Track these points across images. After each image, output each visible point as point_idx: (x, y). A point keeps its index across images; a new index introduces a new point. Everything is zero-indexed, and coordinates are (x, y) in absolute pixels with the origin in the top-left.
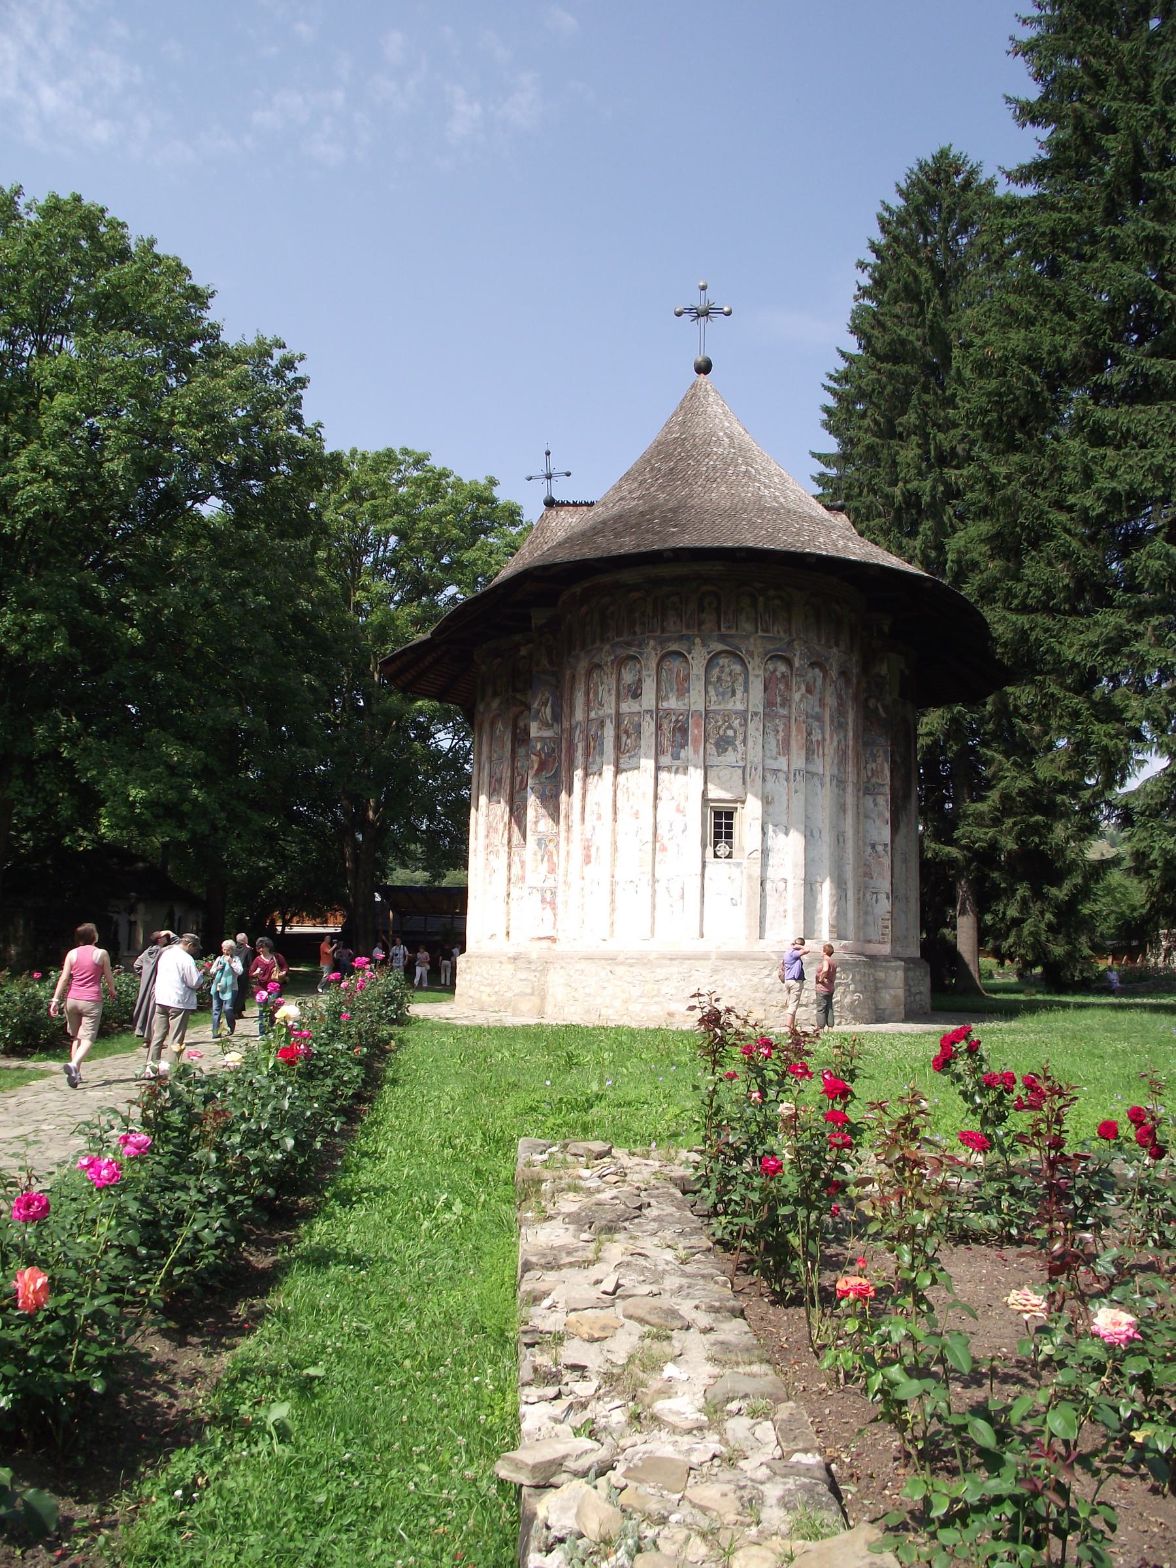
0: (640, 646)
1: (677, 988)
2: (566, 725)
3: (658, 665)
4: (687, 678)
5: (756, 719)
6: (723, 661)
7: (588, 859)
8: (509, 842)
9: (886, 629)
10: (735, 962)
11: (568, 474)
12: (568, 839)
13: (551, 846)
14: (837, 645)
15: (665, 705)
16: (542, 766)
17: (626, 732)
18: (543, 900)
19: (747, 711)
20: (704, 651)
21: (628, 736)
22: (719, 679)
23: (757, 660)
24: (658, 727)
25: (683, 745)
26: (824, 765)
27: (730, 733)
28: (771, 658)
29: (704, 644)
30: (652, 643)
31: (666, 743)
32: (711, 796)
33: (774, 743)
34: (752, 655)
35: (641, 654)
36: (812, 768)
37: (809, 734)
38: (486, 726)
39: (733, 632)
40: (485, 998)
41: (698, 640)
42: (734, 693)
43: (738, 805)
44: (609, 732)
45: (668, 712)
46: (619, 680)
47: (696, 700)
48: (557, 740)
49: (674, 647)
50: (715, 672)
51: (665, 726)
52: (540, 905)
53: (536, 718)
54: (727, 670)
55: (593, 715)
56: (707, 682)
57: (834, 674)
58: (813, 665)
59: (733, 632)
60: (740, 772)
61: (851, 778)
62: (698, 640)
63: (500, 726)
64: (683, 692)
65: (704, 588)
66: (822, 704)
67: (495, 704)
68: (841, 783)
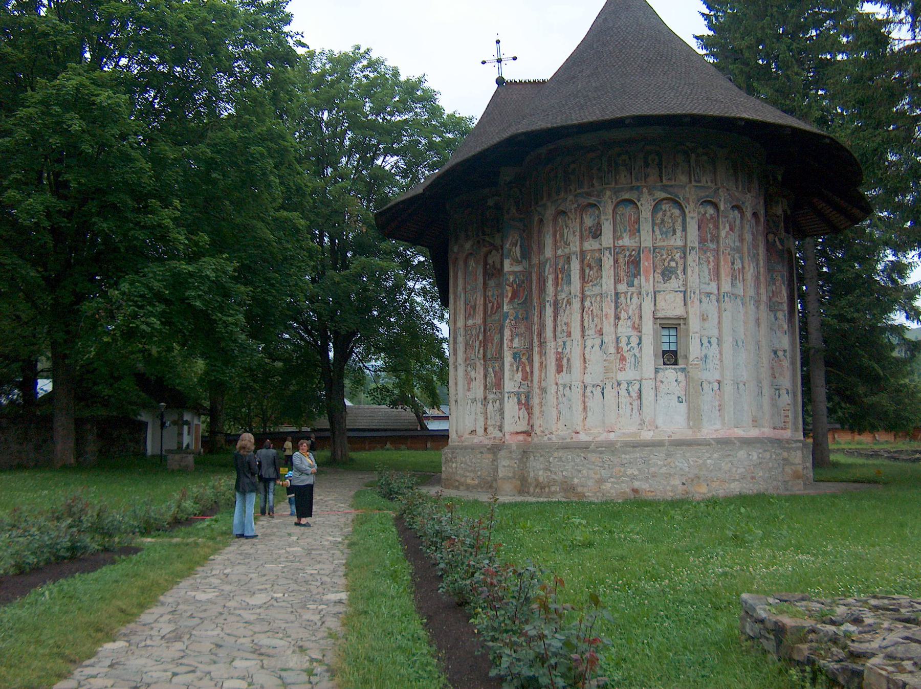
2: (535, 261)
3: (614, 210)
4: (637, 221)
5: (693, 252)
6: (665, 206)
7: (559, 369)
9: (780, 178)
10: (684, 448)
11: (515, 59)
12: (542, 354)
13: (524, 359)
14: (749, 191)
15: (621, 243)
16: (515, 295)
17: (589, 266)
18: (519, 402)
19: (685, 246)
20: (650, 198)
22: (663, 221)
23: (692, 205)
24: (616, 261)
25: (637, 274)
26: (747, 288)
27: (673, 264)
28: (702, 204)
29: (650, 194)
30: (608, 193)
31: (622, 274)
32: (659, 315)
33: (707, 272)
34: (687, 200)
35: (599, 202)
36: (736, 292)
37: (733, 264)
38: (461, 263)
39: (673, 183)
40: (469, 481)
41: (645, 190)
43: (682, 322)
44: (575, 266)
45: (623, 248)
46: (582, 223)
47: (647, 239)
48: (528, 274)
49: (627, 196)
50: (660, 214)
51: (621, 260)
52: (517, 407)
54: (668, 214)
55: (559, 252)
56: (654, 224)
57: (749, 214)
58: (734, 207)
59: (673, 183)
60: (681, 295)
61: (764, 298)
62: (645, 190)
63: (472, 263)
66: (742, 240)
67: (468, 246)
68: (757, 302)
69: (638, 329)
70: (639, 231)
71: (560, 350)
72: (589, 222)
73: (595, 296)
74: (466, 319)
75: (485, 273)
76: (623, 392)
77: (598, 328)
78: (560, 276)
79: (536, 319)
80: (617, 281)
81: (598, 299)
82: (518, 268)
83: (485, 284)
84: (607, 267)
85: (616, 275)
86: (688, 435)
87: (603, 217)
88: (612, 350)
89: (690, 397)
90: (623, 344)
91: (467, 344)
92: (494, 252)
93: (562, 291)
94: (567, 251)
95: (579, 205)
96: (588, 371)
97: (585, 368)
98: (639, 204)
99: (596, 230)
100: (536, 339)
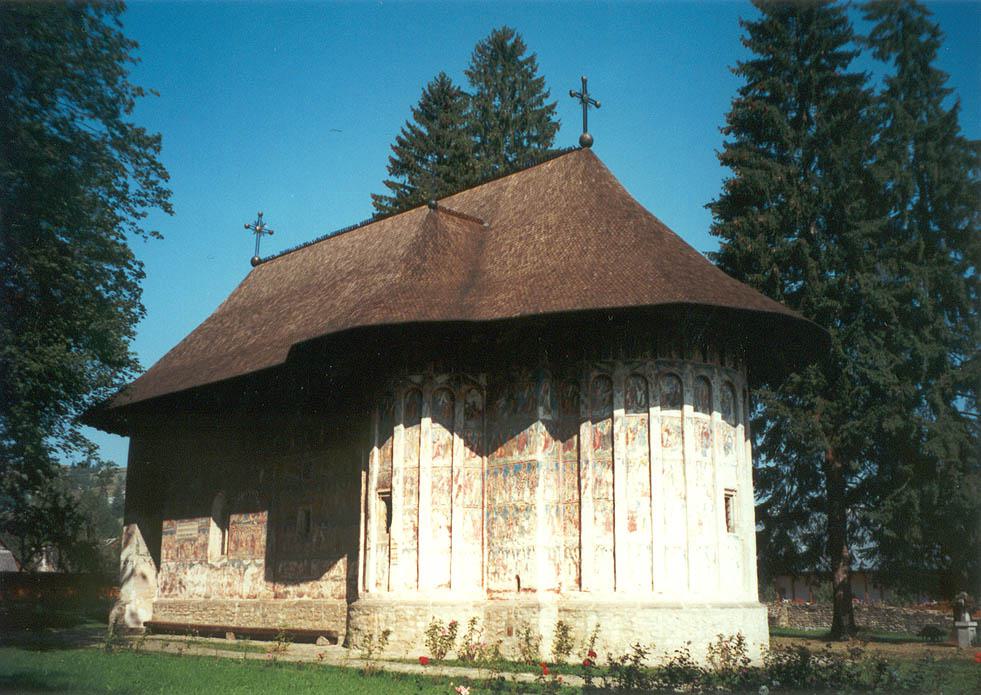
6: (725, 388)
7: (633, 527)
17: (667, 431)
29: (720, 375)
30: (689, 367)
35: (682, 374)
41: (716, 371)
42: (730, 413)
46: (661, 390)
62: (716, 371)
75: (466, 414)
78: (630, 436)
87: (685, 388)
92: (474, 391)
93: (634, 450)
95: (660, 373)
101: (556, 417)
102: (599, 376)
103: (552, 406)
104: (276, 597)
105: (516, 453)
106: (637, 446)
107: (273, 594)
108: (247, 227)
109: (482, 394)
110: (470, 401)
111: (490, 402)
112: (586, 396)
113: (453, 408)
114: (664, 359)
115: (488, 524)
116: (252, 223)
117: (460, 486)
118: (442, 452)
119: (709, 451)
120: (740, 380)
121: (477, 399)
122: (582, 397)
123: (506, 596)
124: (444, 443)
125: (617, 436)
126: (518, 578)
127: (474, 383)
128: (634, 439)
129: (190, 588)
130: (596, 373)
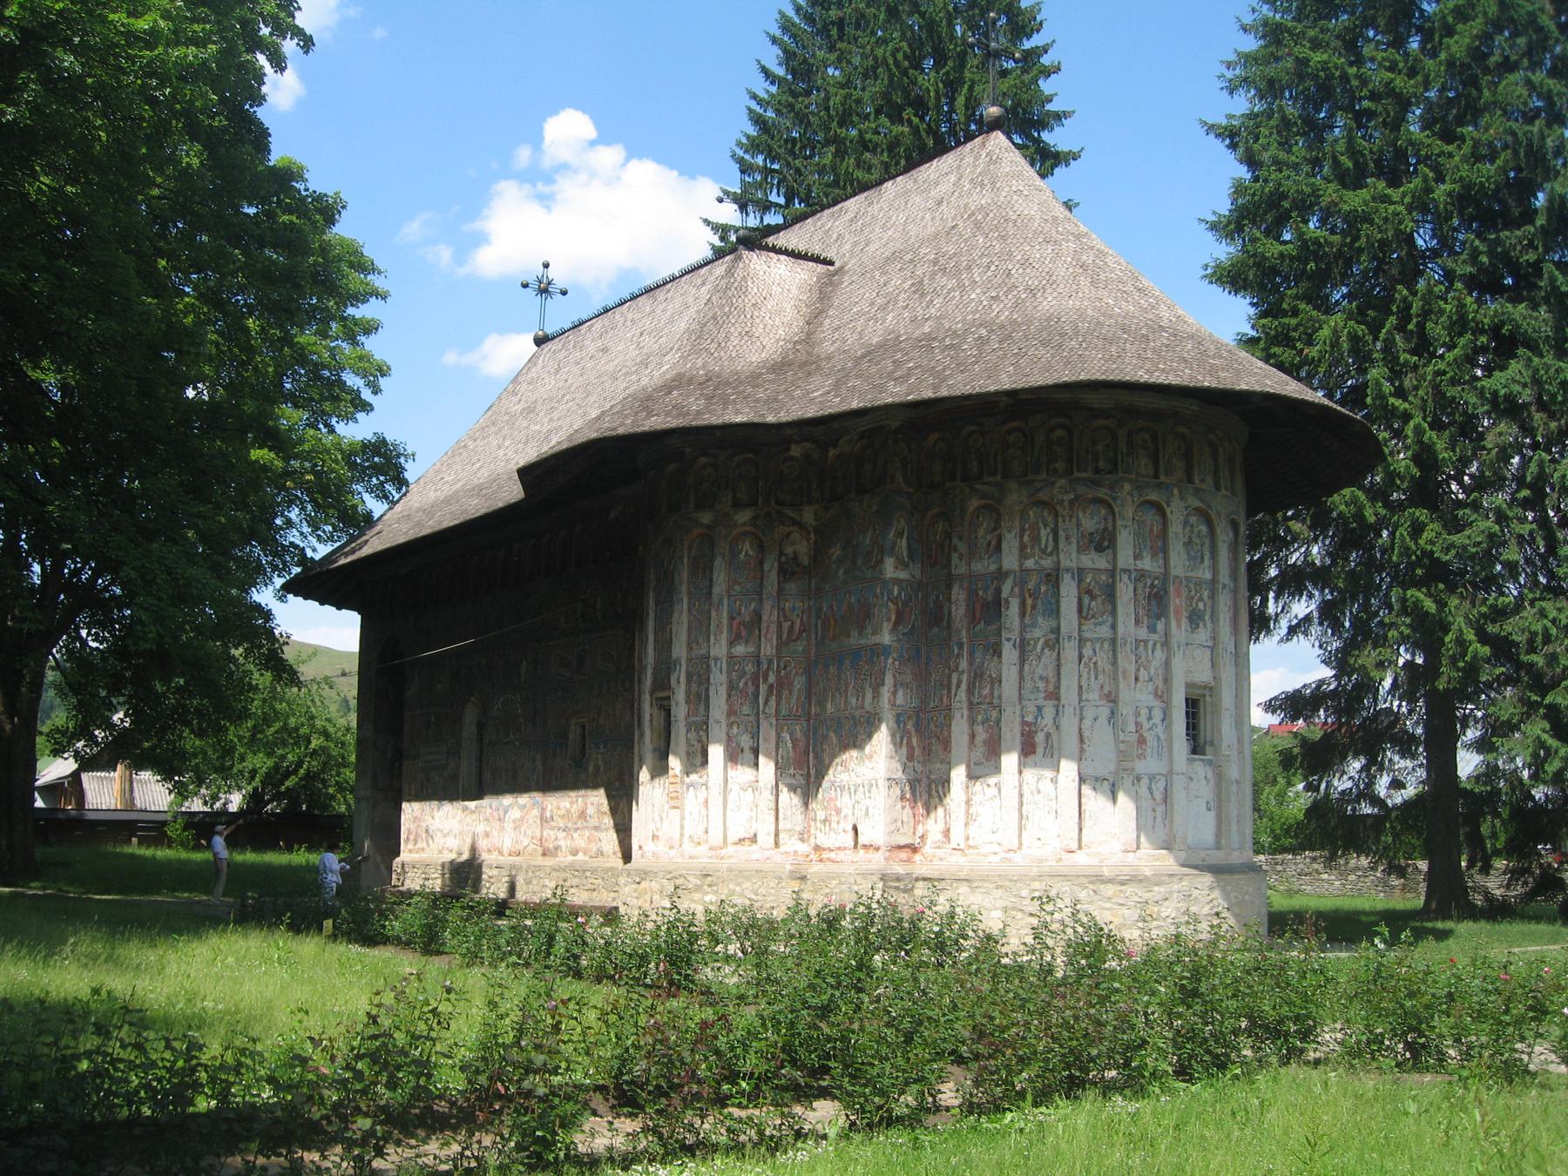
0: (1111, 488)
1: (1178, 909)
6: (1193, 519)
8: (777, 711)
17: (1089, 592)
19: (1214, 581)
21: (1093, 597)
30: (1127, 487)
35: (1115, 499)
41: (1176, 491)
45: (1142, 575)
46: (1079, 525)
49: (1153, 497)
52: (899, 805)
53: (892, 552)
55: (1030, 563)
62: (1176, 491)
64: (1161, 547)
65: (1181, 429)
69: (1163, 696)
70: (1165, 550)
71: (1029, 719)
72: (1090, 522)
73: (1102, 640)
74: (731, 644)
76: (1144, 791)
77: (1106, 690)
78: (1029, 601)
79: (964, 664)
80: (1137, 622)
81: (1106, 645)
82: (903, 575)
83: (780, 591)
84: (1125, 599)
85: (1136, 615)
86: (1217, 857)
87: (1119, 523)
88: (1132, 728)
89: (1219, 804)
90: (1143, 718)
91: (731, 687)
92: (796, 536)
94: (1047, 563)
95: (1077, 497)
96: (1087, 754)
97: (1082, 750)
98: (1168, 511)
99: (1102, 539)
100: (962, 694)
101: (918, 574)
102: (985, 507)
103: (911, 556)
104: (544, 854)
105: (854, 633)
106: (1040, 620)
107: (540, 850)
108: (525, 286)
109: (808, 540)
110: (789, 550)
111: (819, 553)
112: (961, 538)
113: (761, 563)
114: (1085, 475)
115: (815, 745)
116: (531, 279)
117: (771, 686)
118: (744, 633)
119: (1160, 626)
120: (1227, 504)
121: (801, 547)
122: (955, 541)
123: (841, 856)
124: (747, 619)
125: (1007, 602)
126: (855, 829)
127: (794, 522)
128: (1034, 607)
129: (439, 840)
130: (975, 503)
